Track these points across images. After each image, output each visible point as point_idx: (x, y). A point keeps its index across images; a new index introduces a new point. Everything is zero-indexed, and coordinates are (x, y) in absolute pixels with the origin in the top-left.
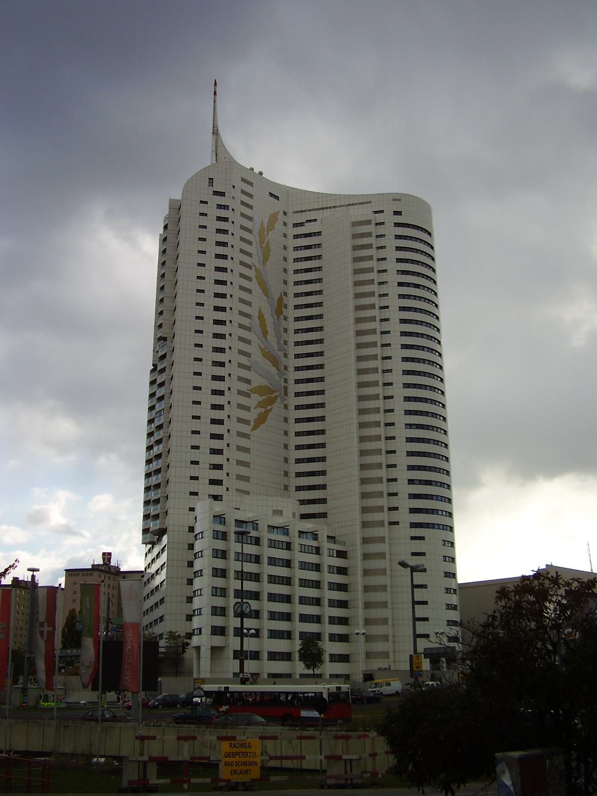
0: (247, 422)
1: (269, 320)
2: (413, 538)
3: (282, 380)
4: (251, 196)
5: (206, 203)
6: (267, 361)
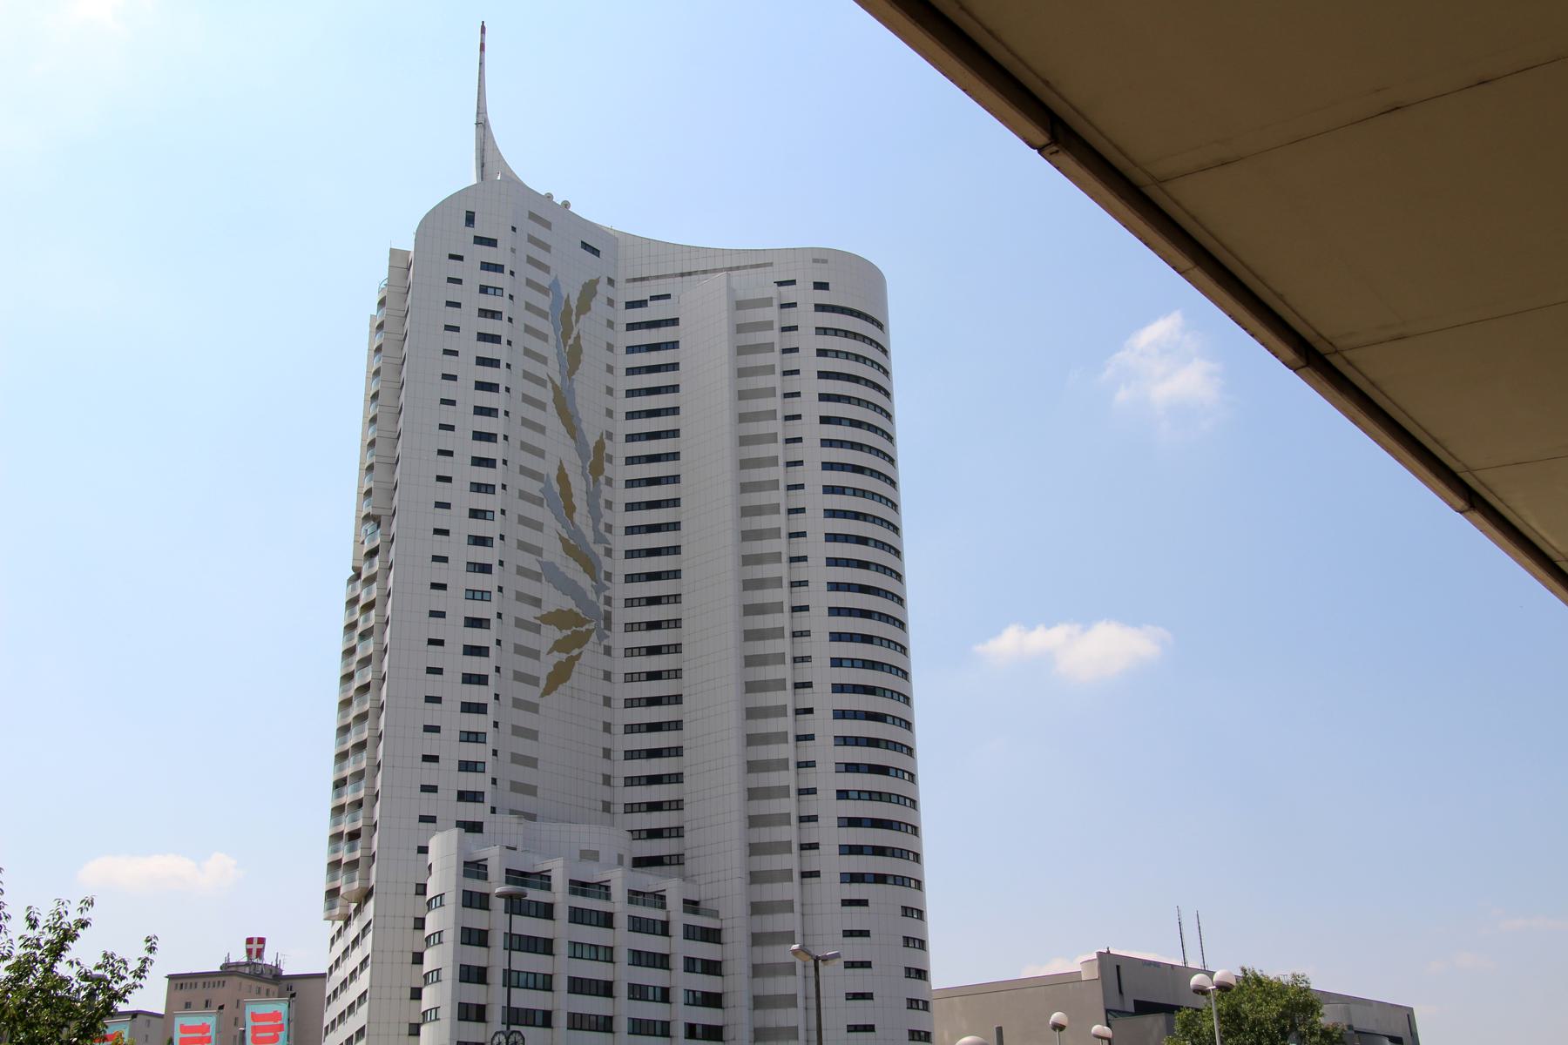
0: (532, 680)
1: (578, 486)
2: (847, 903)
3: (602, 599)
4: (546, 247)
5: (460, 258)
6: (572, 563)
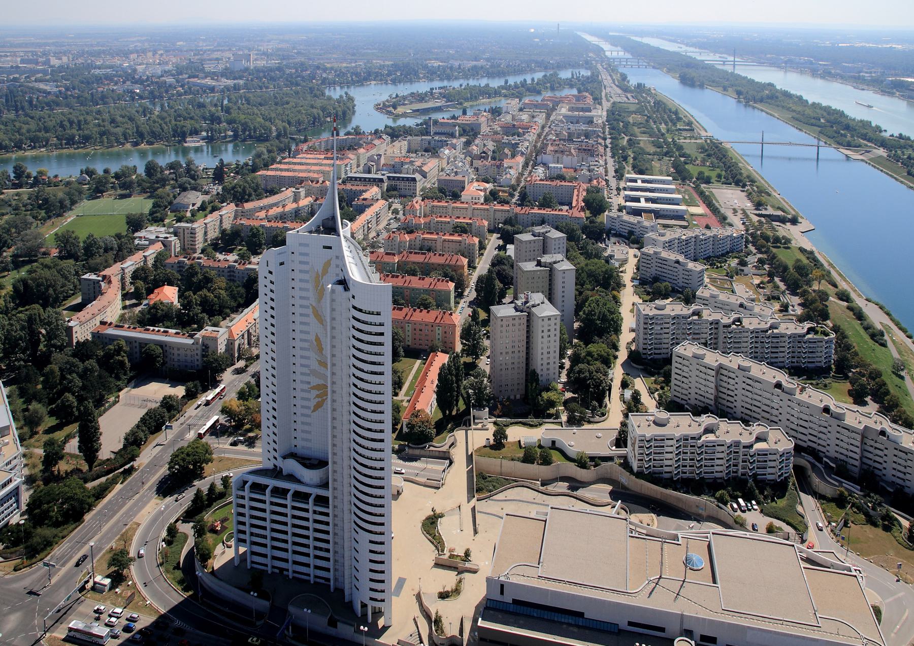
0: (309, 408)
